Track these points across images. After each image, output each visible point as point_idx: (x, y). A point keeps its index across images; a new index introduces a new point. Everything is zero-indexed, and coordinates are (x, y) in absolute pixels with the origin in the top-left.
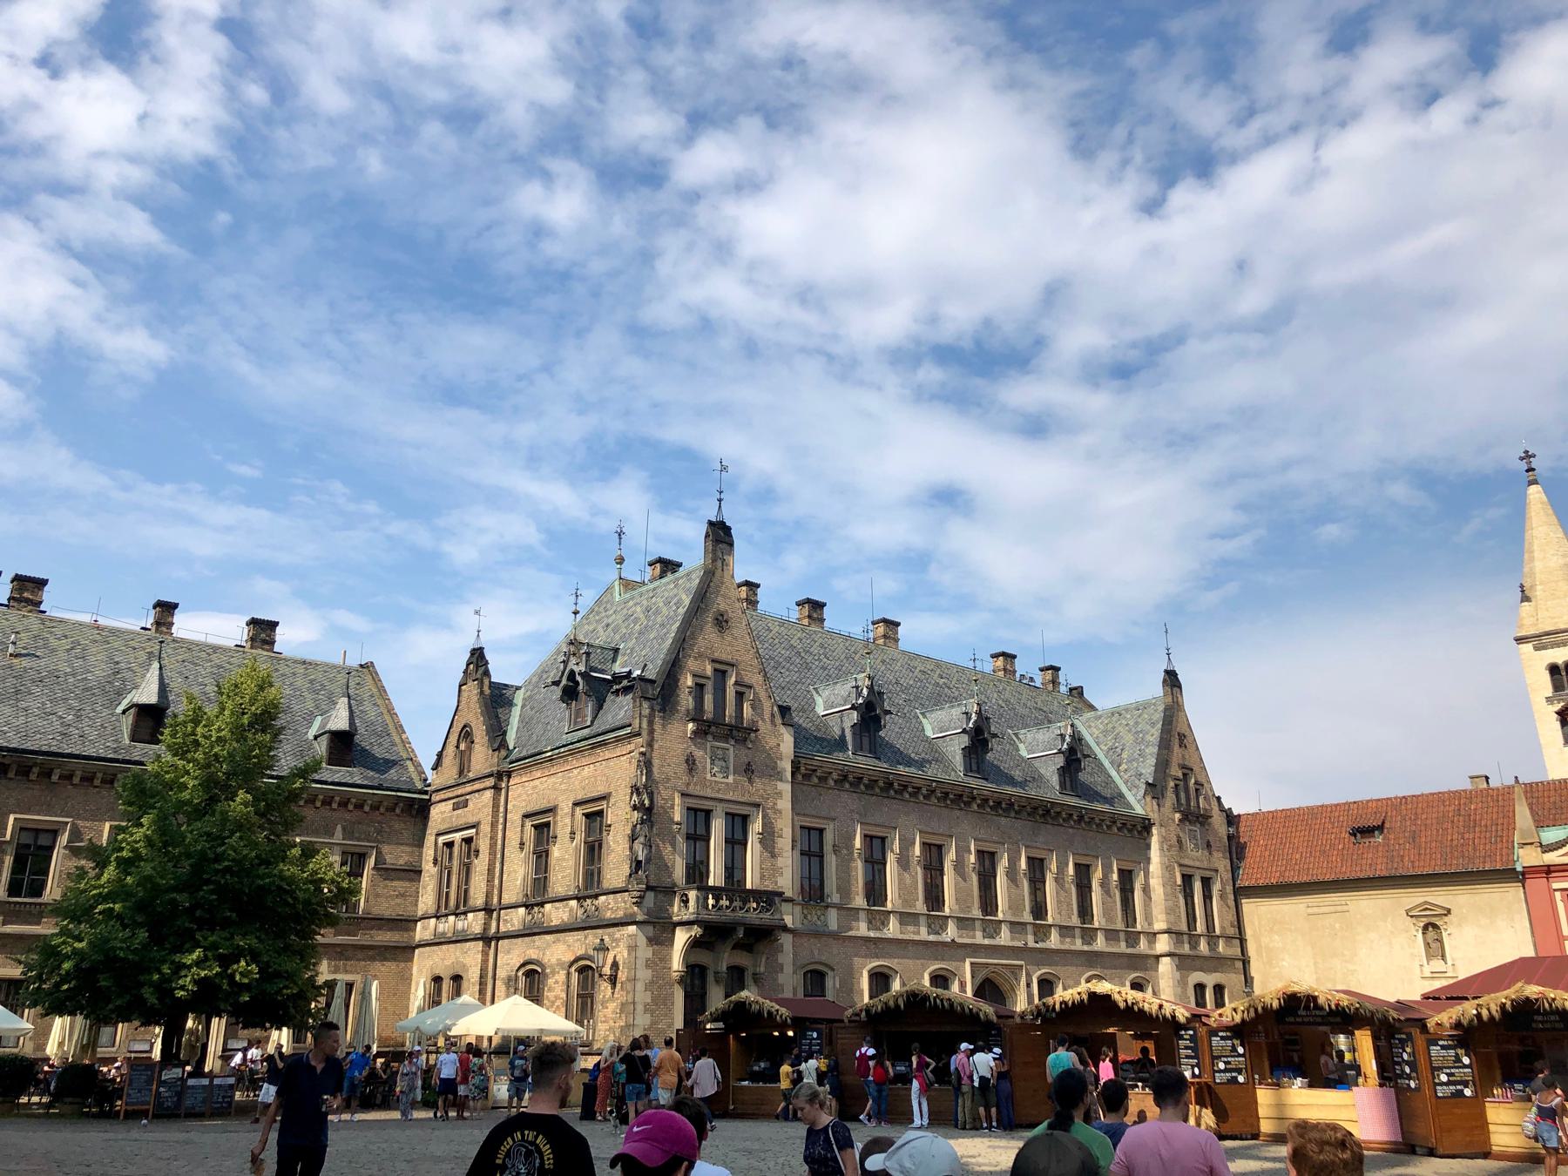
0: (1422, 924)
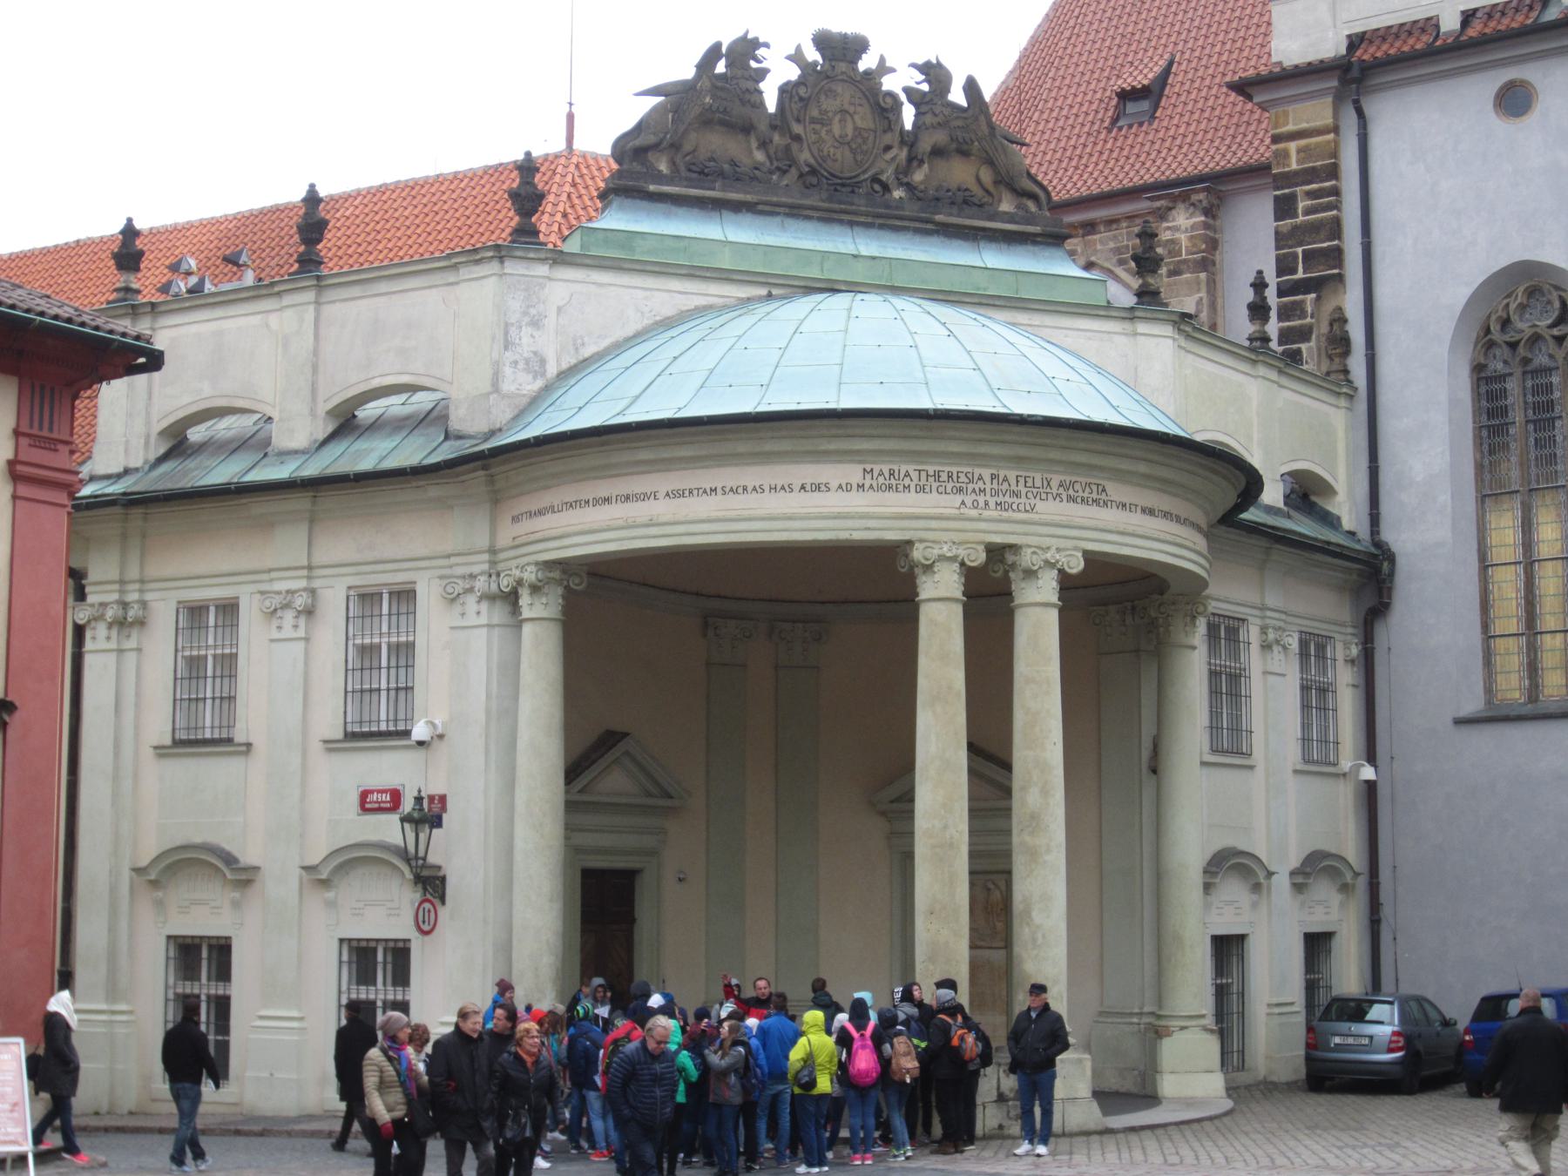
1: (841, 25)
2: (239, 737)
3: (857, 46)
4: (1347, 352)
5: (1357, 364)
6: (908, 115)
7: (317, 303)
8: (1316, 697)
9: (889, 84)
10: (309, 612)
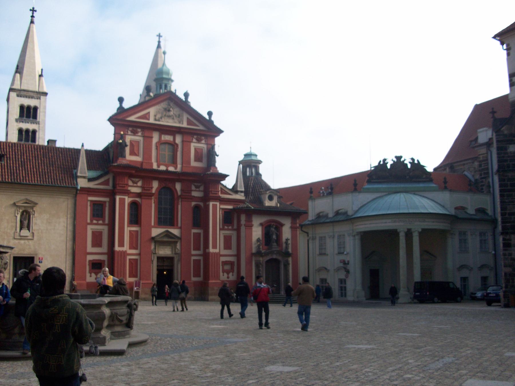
0: (21, 211)
1: (398, 155)
2: (327, 253)
3: (401, 157)
4: (490, 188)
5: (491, 189)
6: (409, 166)
7: (333, 198)
8: (483, 242)
9: (405, 162)
10: (333, 237)
